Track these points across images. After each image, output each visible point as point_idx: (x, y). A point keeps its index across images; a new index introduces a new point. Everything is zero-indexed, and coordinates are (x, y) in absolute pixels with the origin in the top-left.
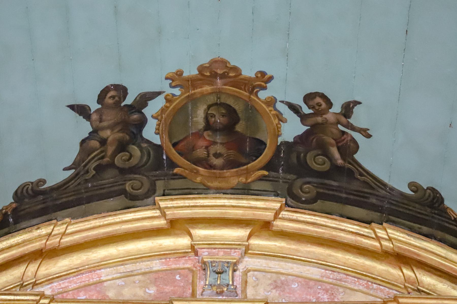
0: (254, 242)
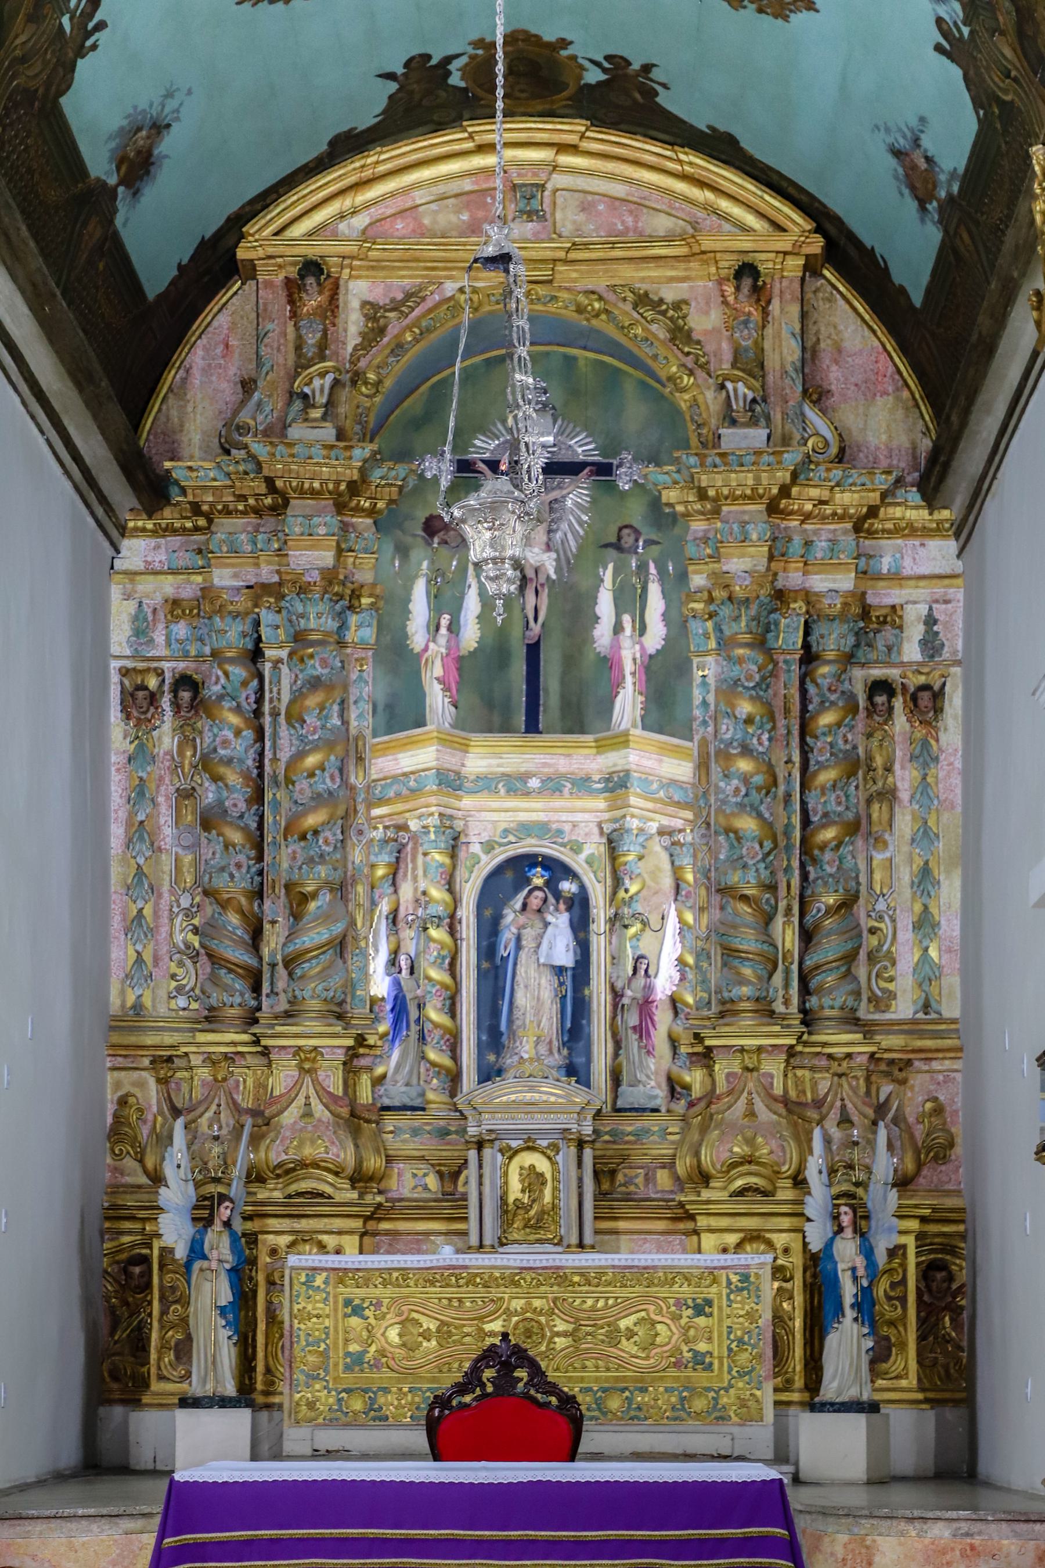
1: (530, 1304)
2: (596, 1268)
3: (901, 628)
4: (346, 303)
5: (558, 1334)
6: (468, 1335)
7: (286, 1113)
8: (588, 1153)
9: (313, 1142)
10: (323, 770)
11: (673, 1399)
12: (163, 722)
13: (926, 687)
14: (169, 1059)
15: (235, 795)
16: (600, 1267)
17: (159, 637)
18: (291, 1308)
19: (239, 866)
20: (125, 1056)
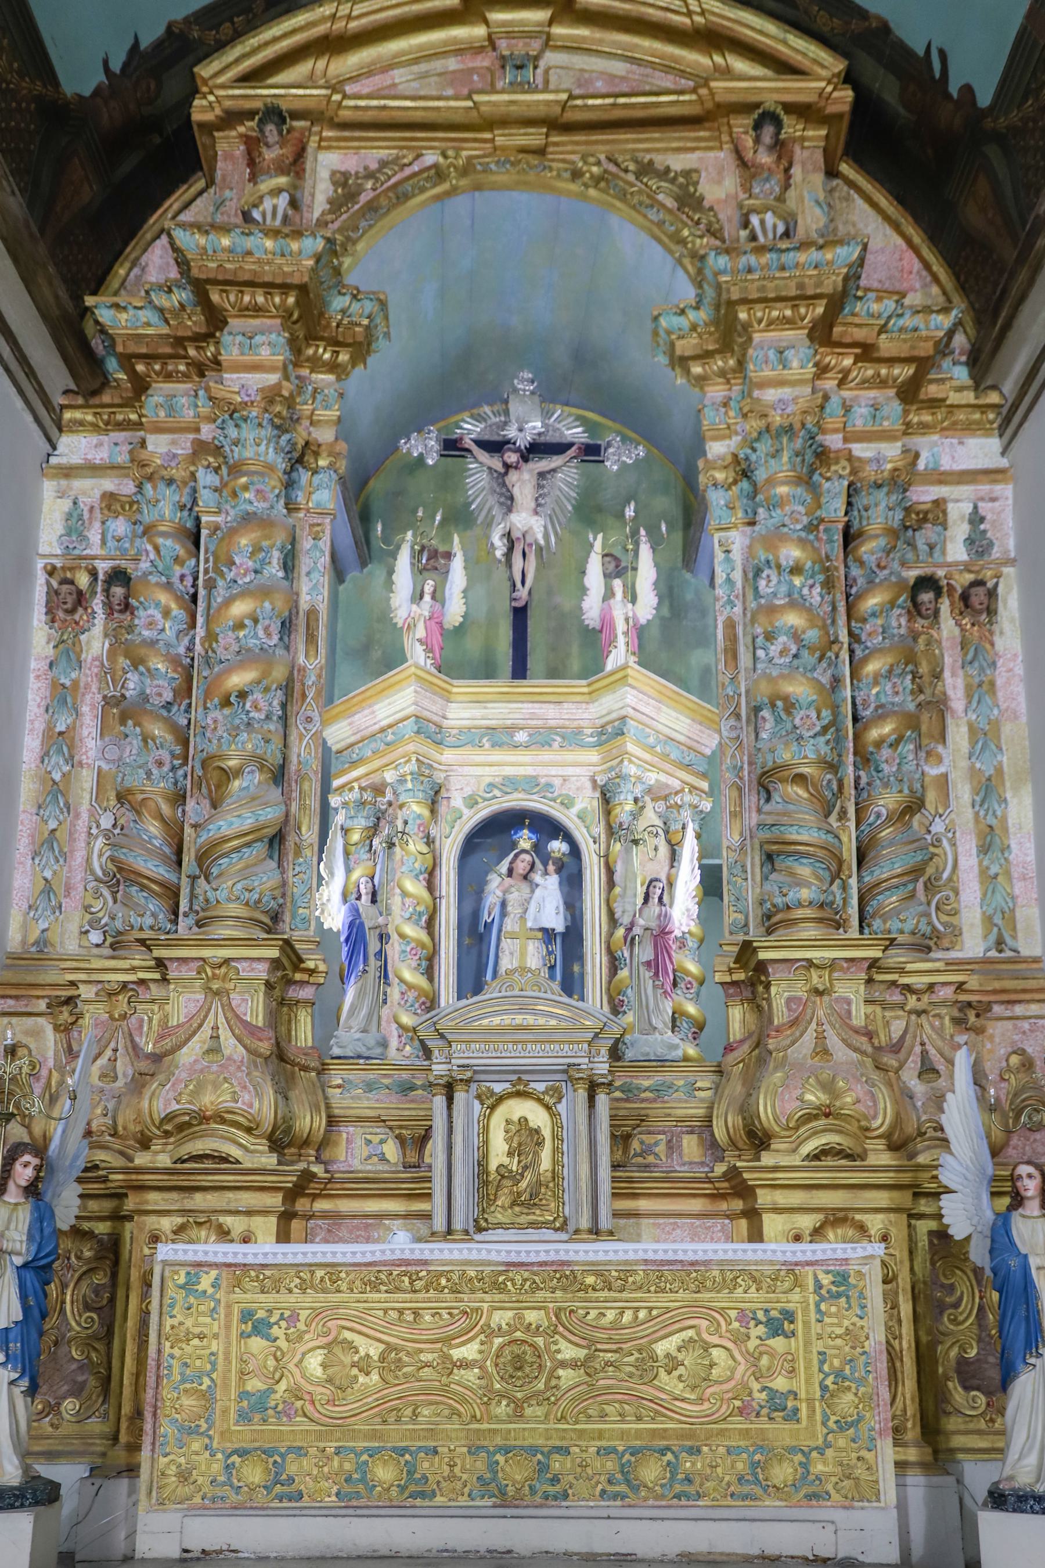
0: (558, 30)
1: (521, 1318)
2: (619, 1263)
3: (944, 526)
4: (314, 171)
5: (563, 1364)
6: (427, 1365)
7: (185, 1050)
8: (602, 1099)
9: (216, 1086)
11: (740, 1466)
12: (94, 625)
13: (979, 583)
14: (70, 1001)
15: (161, 682)
16: (626, 1262)
17: (94, 535)
18: (160, 1325)
20: (16, 998)
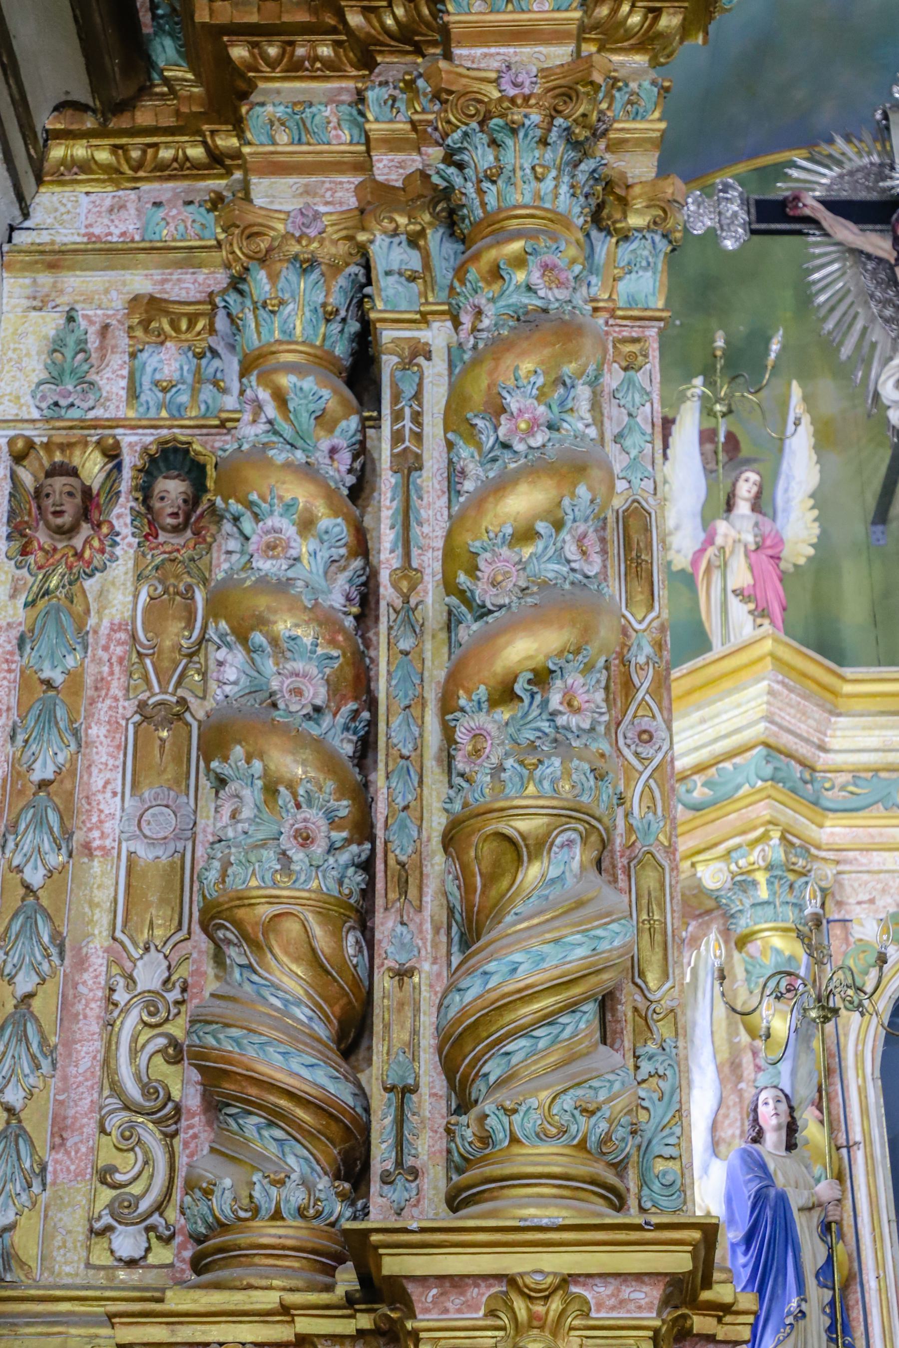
10: (558, 525)
12: (114, 558)
19: (305, 839)
